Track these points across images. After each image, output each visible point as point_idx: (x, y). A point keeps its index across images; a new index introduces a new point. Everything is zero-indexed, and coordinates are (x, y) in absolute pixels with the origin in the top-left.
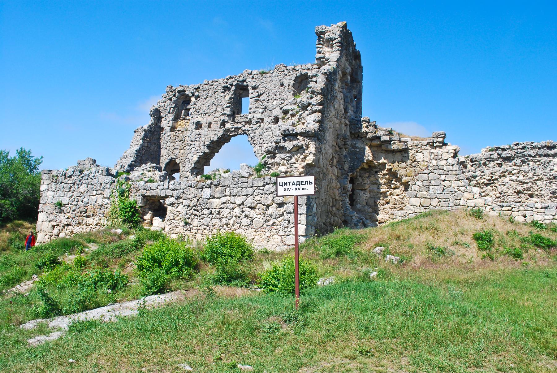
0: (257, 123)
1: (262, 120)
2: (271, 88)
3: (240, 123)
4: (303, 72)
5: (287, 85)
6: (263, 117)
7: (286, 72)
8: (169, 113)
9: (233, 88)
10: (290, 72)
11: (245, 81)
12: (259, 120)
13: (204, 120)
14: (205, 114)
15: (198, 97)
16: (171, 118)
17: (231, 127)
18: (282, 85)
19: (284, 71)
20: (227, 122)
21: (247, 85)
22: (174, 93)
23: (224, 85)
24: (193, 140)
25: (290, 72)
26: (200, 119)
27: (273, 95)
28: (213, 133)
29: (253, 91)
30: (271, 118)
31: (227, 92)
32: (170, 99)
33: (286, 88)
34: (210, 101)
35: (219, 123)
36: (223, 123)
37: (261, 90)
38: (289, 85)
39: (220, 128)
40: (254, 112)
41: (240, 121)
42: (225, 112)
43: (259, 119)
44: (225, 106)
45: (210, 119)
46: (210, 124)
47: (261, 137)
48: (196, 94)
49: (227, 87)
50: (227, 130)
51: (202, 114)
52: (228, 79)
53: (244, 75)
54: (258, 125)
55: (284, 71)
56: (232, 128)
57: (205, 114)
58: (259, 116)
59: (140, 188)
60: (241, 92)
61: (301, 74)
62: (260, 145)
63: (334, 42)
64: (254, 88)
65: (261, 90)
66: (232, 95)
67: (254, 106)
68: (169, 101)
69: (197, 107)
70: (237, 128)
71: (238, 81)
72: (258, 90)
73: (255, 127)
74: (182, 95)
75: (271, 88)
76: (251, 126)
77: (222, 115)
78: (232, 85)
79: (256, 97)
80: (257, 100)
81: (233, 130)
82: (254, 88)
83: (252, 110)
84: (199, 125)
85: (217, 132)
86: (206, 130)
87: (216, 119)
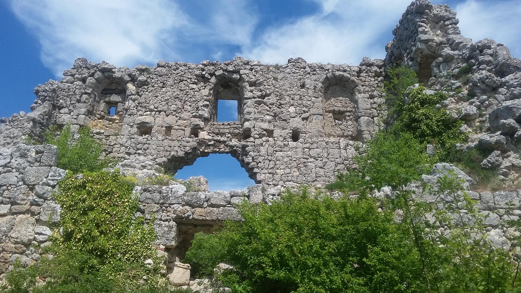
0: (261, 136)
1: (270, 133)
2: (284, 87)
3: (222, 134)
4: (337, 73)
5: (312, 87)
6: (272, 128)
7: (308, 69)
8: (79, 101)
9: (213, 80)
10: (315, 70)
11: (237, 72)
12: (264, 132)
13: (158, 121)
14: (160, 112)
15: (145, 83)
16: (83, 110)
17: (210, 137)
18: (303, 86)
19: (304, 68)
20: (202, 129)
21: (241, 79)
22: (92, 71)
23: (198, 72)
24: (132, 151)
25: (315, 70)
26: (148, 119)
27: (288, 99)
28: (176, 143)
29: (252, 88)
30: (287, 131)
31: (202, 84)
32: (84, 80)
33: (311, 92)
34: (169, 92)
35: (188, 130)
36: (195, 131)
37: (268, 88)
38: (315, 87)
39: (190, 137)
40: (256, 119)
41: (221, 131)
42: (200, 112)
43: (265, 130)
44: (201, 104)
45: (171, 120)
46: (169, 129)
47: (270, 158)
48: (142, 78)
49: (203, 77)
50: (202, 143)
51: (151, 111)
52: (205, 65)
53: (235, 63)
54: (264, 139)
55: (304, 68)
56: (210, 140)
57: (160, 112)
58: (265, 126)
59: (172, 200)
60: (221, 89)
61: (334, 75)
62: (270, 171)
63: (446, 23)
64: (252, 84)
65: (268, 88)
66: (210, 90)
67: (256, 111)
68: (80, 83)
69: (142, 100)
70: (219, 141)
71: (226, 70)
72: (261, 87)
73: (258, 142)
74: (106, 77)
75: (284, 87)
76: (252, 139)
77: (194, 117)
78: (212, 75)
79: (259, 97)
80: (259, 103)
81: (212, 143)
82: (252, 84)
83: (252, 116)
84: (145, 129)
85: (185, 144)
86: (160, 138)
87: (180, 122)
